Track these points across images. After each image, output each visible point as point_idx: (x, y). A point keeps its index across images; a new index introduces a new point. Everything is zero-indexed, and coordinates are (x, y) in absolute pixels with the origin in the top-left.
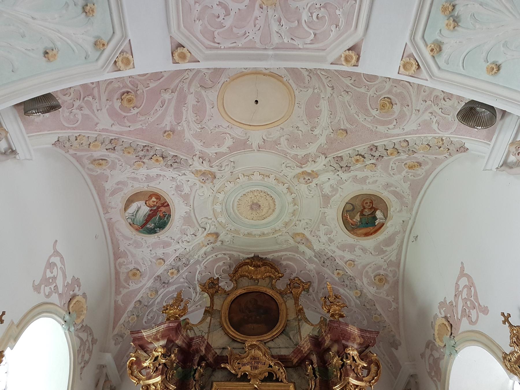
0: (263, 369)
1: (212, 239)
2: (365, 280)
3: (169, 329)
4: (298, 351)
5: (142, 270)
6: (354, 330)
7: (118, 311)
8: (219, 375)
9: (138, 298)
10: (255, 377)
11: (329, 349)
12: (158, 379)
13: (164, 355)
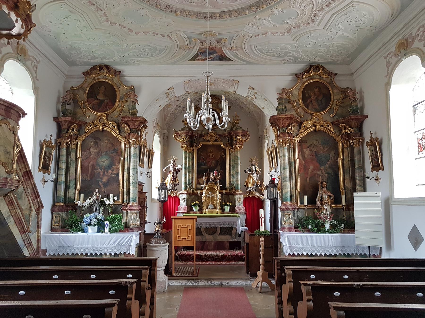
0: (214, 139)
1: (195, 95)
3: (186, 132)
4: (224, 134)
5: (171, 104)
6: (240, 131)
7: (165, 116)
8: (201, 140)
9: (171, 112)
10: (212, 141)
11: (233, 135)
12: (186, 145)
13: (186, 138)
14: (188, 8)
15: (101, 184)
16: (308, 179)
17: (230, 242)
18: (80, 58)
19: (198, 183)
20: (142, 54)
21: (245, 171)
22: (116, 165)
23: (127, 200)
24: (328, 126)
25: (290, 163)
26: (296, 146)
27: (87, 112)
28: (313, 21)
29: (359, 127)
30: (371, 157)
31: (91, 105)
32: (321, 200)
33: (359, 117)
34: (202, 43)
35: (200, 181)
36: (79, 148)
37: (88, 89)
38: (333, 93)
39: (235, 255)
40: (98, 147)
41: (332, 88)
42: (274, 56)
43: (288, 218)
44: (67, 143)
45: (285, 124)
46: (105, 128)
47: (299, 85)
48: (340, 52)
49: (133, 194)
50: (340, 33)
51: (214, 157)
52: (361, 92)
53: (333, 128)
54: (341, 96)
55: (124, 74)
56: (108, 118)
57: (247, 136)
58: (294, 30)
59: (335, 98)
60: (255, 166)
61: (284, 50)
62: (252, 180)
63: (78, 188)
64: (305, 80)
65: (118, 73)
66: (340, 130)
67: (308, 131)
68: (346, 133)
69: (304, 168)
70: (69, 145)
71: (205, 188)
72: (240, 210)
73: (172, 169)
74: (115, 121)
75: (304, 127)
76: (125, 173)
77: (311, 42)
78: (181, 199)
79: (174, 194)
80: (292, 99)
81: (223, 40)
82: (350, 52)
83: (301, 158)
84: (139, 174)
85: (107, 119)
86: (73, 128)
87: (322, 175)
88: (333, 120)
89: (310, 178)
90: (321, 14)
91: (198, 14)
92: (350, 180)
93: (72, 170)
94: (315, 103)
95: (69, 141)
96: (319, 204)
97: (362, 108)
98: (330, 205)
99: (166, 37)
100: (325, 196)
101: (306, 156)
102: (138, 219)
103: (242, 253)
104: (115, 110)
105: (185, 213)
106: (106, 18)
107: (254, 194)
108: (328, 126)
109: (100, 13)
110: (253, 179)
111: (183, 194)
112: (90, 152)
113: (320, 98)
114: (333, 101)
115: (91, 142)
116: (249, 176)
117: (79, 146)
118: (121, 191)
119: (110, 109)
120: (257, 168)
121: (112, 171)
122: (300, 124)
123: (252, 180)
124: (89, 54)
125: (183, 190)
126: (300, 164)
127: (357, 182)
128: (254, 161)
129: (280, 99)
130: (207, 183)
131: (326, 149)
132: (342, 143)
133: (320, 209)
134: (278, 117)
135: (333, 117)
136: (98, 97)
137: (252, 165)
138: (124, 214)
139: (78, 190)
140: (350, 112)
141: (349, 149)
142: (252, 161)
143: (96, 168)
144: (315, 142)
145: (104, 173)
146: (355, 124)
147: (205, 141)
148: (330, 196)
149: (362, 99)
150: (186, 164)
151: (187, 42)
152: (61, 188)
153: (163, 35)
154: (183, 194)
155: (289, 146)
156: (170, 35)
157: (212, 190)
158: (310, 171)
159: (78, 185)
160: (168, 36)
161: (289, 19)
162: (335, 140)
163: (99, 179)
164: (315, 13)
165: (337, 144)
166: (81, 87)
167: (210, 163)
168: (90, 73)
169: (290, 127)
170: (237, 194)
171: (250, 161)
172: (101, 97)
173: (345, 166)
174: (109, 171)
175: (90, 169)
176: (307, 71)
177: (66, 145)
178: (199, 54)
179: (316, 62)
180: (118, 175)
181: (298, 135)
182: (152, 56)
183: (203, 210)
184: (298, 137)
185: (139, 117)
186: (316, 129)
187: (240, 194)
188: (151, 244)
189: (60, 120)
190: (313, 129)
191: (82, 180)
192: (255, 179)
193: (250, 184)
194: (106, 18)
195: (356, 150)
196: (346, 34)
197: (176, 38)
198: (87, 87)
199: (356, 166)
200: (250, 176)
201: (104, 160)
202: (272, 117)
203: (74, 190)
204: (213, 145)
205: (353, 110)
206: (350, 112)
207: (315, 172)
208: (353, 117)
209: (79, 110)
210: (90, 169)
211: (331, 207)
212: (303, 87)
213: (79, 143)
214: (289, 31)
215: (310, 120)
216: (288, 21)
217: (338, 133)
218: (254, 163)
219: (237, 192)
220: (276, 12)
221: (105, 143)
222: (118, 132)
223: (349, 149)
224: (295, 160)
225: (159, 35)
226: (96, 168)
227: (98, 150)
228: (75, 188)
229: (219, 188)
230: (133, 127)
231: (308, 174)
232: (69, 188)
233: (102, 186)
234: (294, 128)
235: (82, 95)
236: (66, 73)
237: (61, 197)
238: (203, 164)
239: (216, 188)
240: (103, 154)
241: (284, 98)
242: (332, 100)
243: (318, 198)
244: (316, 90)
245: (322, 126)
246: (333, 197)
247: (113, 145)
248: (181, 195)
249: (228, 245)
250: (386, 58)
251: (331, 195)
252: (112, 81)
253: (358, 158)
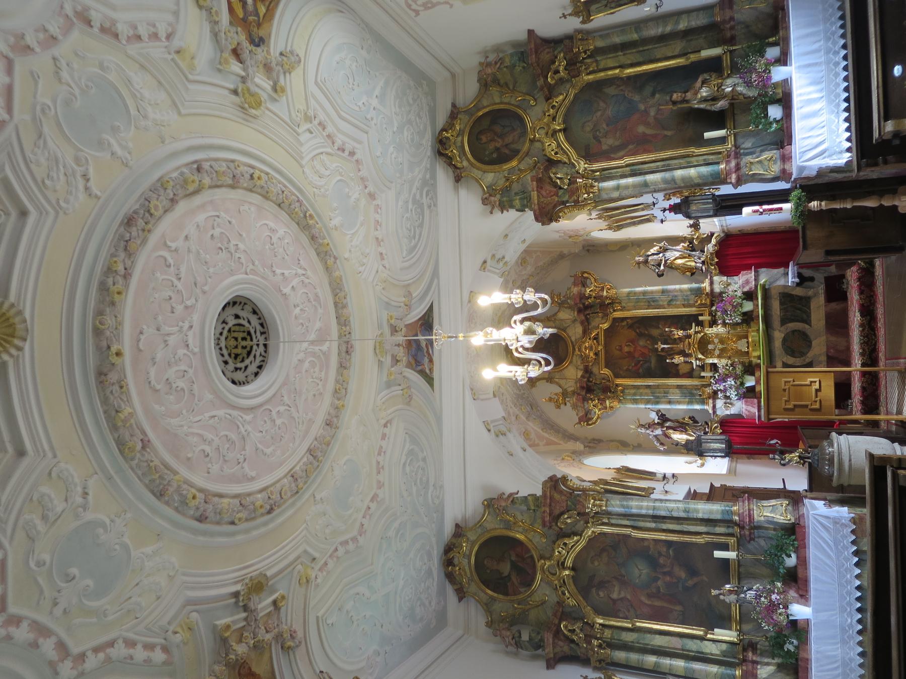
2: (524, 273)
6: (575, 290)
12: (607, 402)
14: (331, 385)
15: (690, 583)
16: (666, 133)
17: (829, 299)
18: (430, 603)
19: (690, 375)
20: (421, 479)
21: (659, 276)
22: (648, 547)
23: (728, 527)
24: (553, 107)
25: (633, 174)
26: (596, 166)
27: (537, 598)
28: (352, 154)
29: (552, 45)
30: (613, 8)
31: (522, 590)
32: (714, 99)
33: (533, 46)
34: (398, 361)
35: (684, 369)
36: (612, 623)
37: (489, 592)
38: (488, 106)
39: (860, 287)
40: (608, 582)
41: (479, 110)
42: (421, 225)
43: (758, 166)
44: (600, 646)
45: (551, 192)
46: (569, 563)
47: (477, 173)
48: (411, 101)
49: (715, 509)
50: (375, 102)
51: (632, 341)
52: (485, 53)
53: (557, 96)
54: (494, 90)
55: (460, 517)
56: (547, 555)
57: (585, 275)
58: (371, 188)
59: (497, 100)
60: (649, 256)
61: (410, 206)
62: (679, 261)
63: (701, 633)
64: (465, 163)
65: (459, 531)
66: (561, 81)
67: (566, 146)
68: (565, 69)
69: (643, 144)
70: (604, 642)
71: (700, 359)
72: (747, 282)
73: (658, 432)
74: (554, 542)
75: (556, 153)
76: (665, 526)
77: (393, 156)
78: (728, 412)
79: (716, 427)
80: (501, 183)
81: (392, 322)
82: (412, 83)
83: (621, 154)
84: (668, 497)
85: (549, 559)
86: (569, 631)
87: (657, 106)
88: (541, 99)
89: (667, 130)
90: (340, 139)
91: (343, 366)
92: (666, 46)
93: (659, 641)
94: (509, 139)
95: (595, 642)
96: (722, 104)
97: (515, 45)
98: (724, 79)
99: (386, 430)
100: (704, 92)
101: (617, 143)
102: (773, 502)
103: (854, 268)
104: (531, 541)
105: (759, 402)
106: (351, 543)
107: (711, 254)
108: (553, 107)
109: (341, 551)
110: (676, 259)
111: (714, 407)
112: (621, 599)
113: (498, 129)
114: (506, 103)
115: (598, 595)
116: (671, 268)
117: (607, 623)
118: (708, 539)
119: (528, 550)
121: (660, 554)
122: (551, 163)
123: (679, 261)
124: (423, 585)
125: (706, 407)
126: (634, 153)
127: (668, 29)
128: (637, 259)
129: (503, 208)
130: (689, 355)
131: (602, 104)
132: (588, 74)
133: (733, 99)
134: (536, 207)
135: (535, 100)
136: (506, 574)
138: (762, 535)
139: (706, 634)
140: (524, 67)
141: (598, 58)
142: (639, 263)
143: (654, 591)
144: (588, 129)
145: (665, 574)
146: (548, 53)
147: (596, 361)
148: (703, 83)
149: (497, 49)
150: (648, 402)
151: (397, 390)
152: (701, 670)
153: (384, 436)
154: (714, 407)
155: (596, 180)
156: (383, 422)
157: (704, 345)
158: (649, 131)
159: (694, 632)
160: (385, 426)
161: (349, 197)
162: (582, 90)
163: (680, 585)
164: (339, 149)
165: (590, 86)
166: (487, 607)
167: (646, 351)
168: (459, 586)
169: (558, 181)
170: (712, 290)
171: (639, 267)
172: (506, 568)
173: (635, 61)
174: (661, 561)
175: (658, 603)
176: (449, 161)
177: (604, 649)
178: (419, 368)
179: (432, 147)
180: (669, 544)
181: (573, 164)
182: (424, 460)
183: (750, 362)
184: (579, 163)
185: (544, 492)
186: (560, 130)
187: (712, 283)
188: (835, 474)
189: (552, 655)
190: (561, 137)
191: (683, 622)
192: (677, 254)
193: (689, 263)
194: (351, 543)
195: (600, 43)
196: (377, 92)
197: (389, 412)
198: (486, 594)
199: (635, 36)
200: (671, 267)
201: (636, 572)
202: (537, 219)
203: (706, 642)
204: (606, 346)
205: (519, 60)
206: (524, 67)
207: (651, 120)
208: (533, 58)
209: (533, 615)
210: (658, 603)
211: (729, 76)
212: (478, 164)
213: (601, 621)
214: (372, 196)
215: (543, 143)
216: (353, 199)
217: (568, 86)
218: (641, 259)
219: (708, 289)
220: (336, 221)
221: (600, 567)
222: (575, 538)
223: (598, 58)
224: (627, 166)
225: (384, 444)
226: (654, 591)
227: (615, 583)
228: (702, 639)
229: (698, 329)
230: (565, 504)
231: (654, 136)
232: (702, 653)
233: (695, 580)
234: (560, 175)
235: (503, 605)
236: (460, 632)
237: (723, 674)
238: (646, 365)
239: (699, 336)
240: (623, 572)
241: (500, 199)
242: (502, 107)
243: (708, 108)
244: (484, 139)
245: (554, 119)
246: (706, 76)
247: (603, 550)
248: (719, 412)
249: (834, 306)
250: (417, 13)
251: (700, 80)
252: (473, 544)
253: (618, 36)
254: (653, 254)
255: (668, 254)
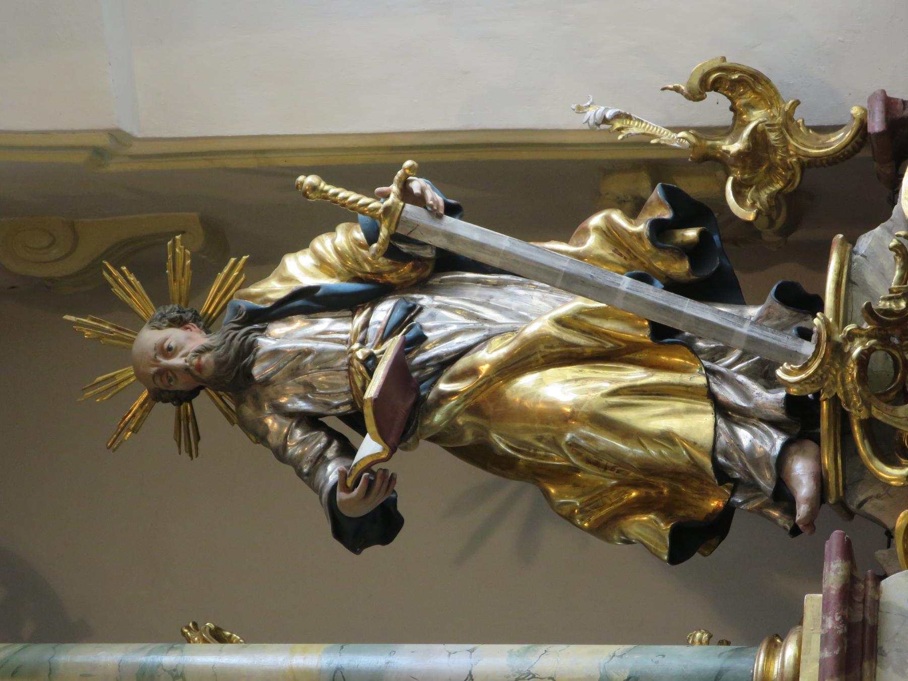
62: (557, 389)
110: (533, 356)
120: (300, 269)
123: (557, 389)
128: (150, 337)
137: (235, 379)
142: (174, 390)
171: (188, 434)
192: (540, 311)
193: (654, 418)
200: (501, 452)
218: (188, 343)
254: (307, 302)
255: (445, 318)
